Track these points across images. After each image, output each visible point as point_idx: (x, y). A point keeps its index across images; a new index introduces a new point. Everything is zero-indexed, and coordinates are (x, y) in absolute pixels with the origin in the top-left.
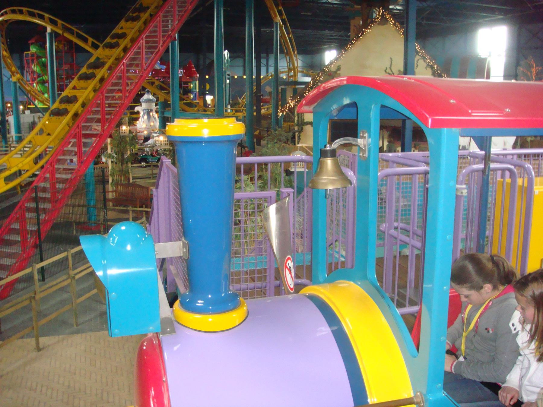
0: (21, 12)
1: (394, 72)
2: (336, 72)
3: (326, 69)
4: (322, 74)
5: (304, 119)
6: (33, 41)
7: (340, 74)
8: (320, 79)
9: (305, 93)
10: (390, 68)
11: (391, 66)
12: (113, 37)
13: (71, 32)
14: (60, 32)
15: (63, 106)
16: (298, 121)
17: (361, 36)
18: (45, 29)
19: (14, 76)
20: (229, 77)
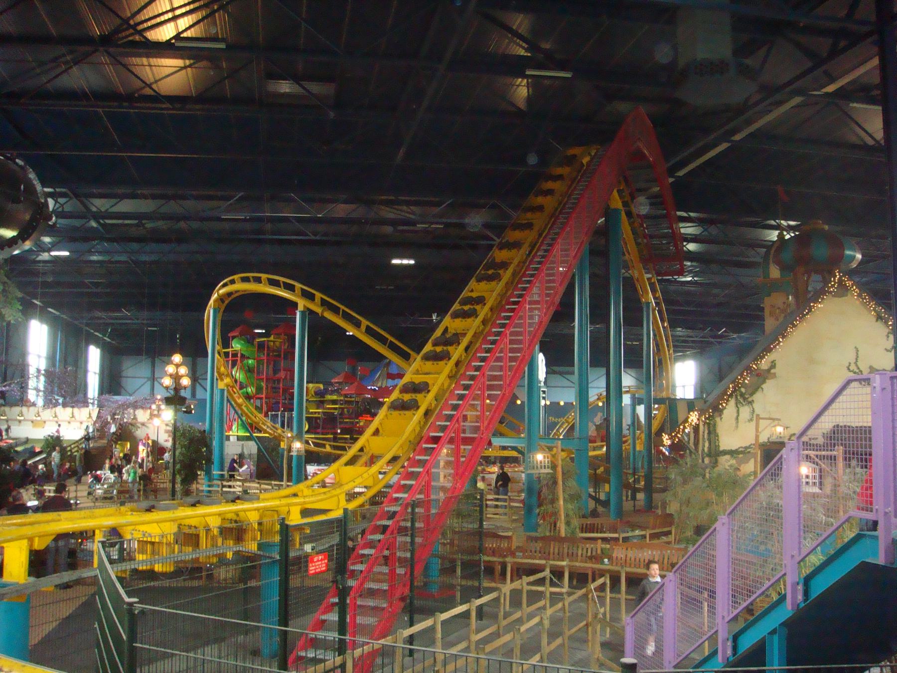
0: (258, 280)
1: (861, 368)
2: (769, 371)
3: (754, 366)
4: (747, 373)
5: (719, 446)
6: (237, 334)
7: (775, 374)
8: (744, 381)
9: (721, 404)
10: (856, 363)
11: (856, 359)
12: (465, 302)
13: (335, 310)
14: (318, 310)
15: (407, 397)
16: (709, 448)
17: (807, 314)
18: (295, 305)
19: (222, 380)
20: (544, 395)
